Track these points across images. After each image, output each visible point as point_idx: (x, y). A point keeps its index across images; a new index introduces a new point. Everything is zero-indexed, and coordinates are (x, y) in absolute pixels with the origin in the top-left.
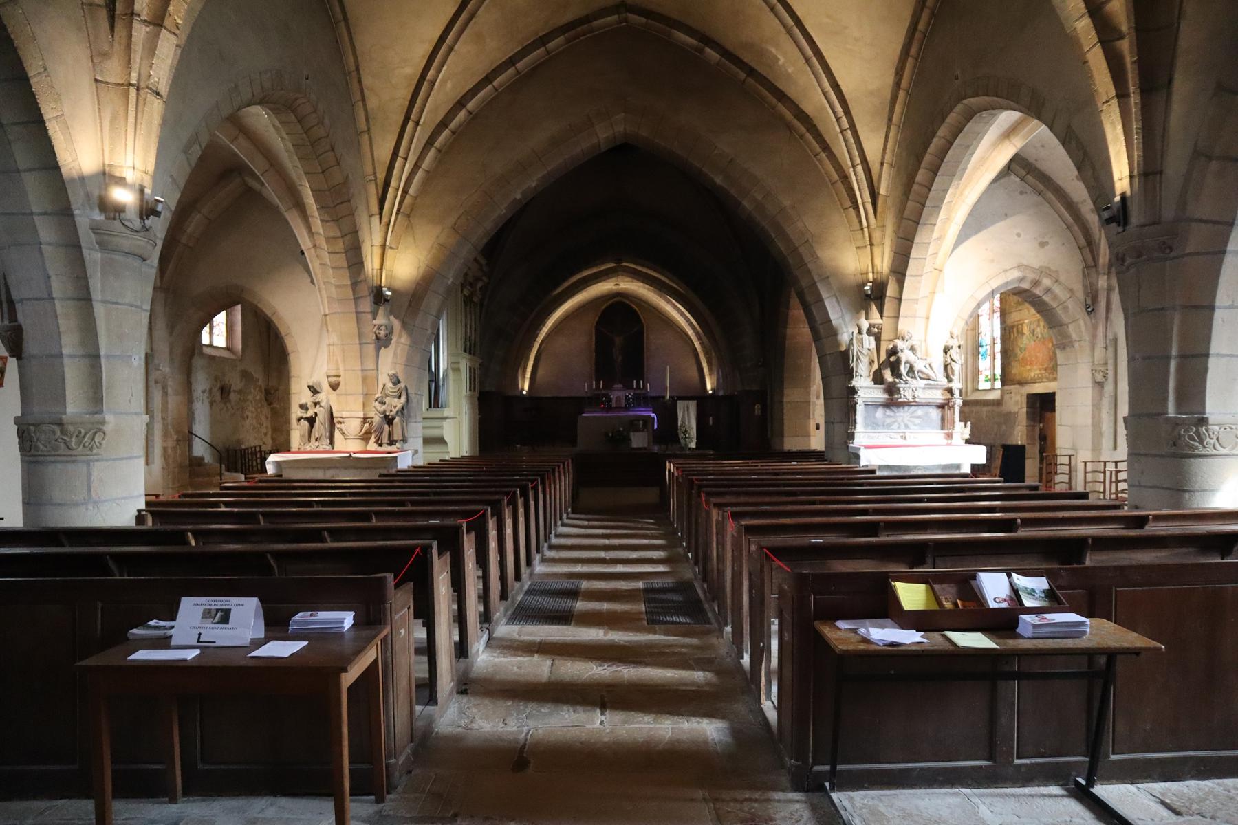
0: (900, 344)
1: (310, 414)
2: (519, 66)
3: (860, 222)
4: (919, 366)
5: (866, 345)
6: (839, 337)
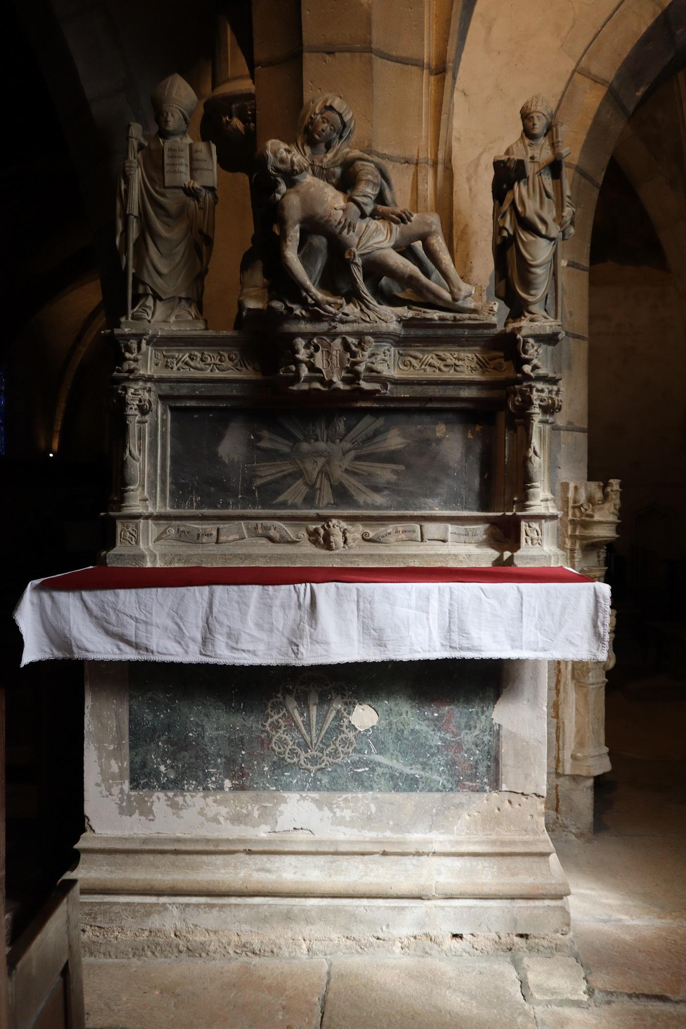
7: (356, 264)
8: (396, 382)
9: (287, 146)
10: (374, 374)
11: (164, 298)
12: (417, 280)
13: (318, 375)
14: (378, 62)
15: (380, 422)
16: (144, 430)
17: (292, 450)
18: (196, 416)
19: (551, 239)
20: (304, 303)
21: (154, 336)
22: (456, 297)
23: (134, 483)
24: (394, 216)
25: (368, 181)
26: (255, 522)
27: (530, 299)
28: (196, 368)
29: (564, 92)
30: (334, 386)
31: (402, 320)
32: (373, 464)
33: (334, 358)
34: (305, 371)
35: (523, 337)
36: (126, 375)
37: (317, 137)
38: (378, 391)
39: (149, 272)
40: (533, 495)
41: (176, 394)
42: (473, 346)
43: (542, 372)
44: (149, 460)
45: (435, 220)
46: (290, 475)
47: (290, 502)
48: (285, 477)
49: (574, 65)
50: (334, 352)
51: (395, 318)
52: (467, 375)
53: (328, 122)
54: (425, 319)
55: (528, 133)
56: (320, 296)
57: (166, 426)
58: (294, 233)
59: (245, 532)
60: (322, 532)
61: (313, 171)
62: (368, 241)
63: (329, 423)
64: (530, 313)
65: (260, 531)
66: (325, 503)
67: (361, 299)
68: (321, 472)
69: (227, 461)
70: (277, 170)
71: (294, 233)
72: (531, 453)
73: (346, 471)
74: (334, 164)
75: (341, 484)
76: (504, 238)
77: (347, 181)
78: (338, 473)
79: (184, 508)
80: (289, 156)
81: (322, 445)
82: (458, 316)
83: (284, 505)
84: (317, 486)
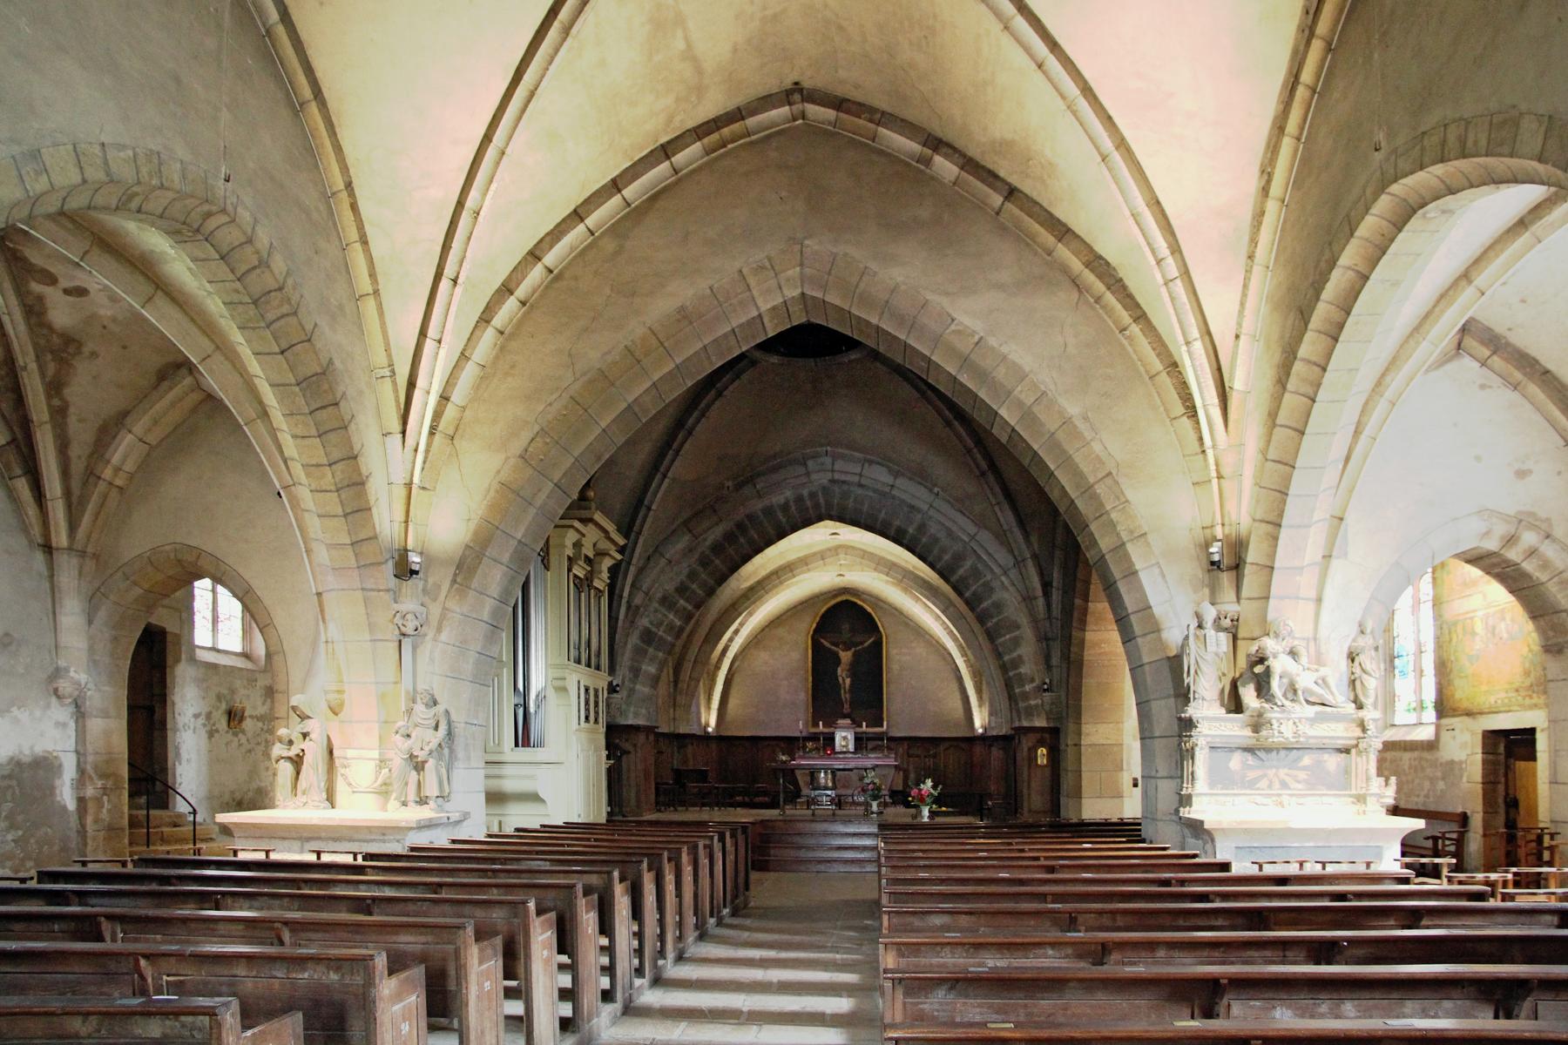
0: (1270, 644)
1: (293, 752)
2: (628, 192)
3: (1201, 439)
4: (1305, 681)
5: (1211, 648)
6: (1165, 635)
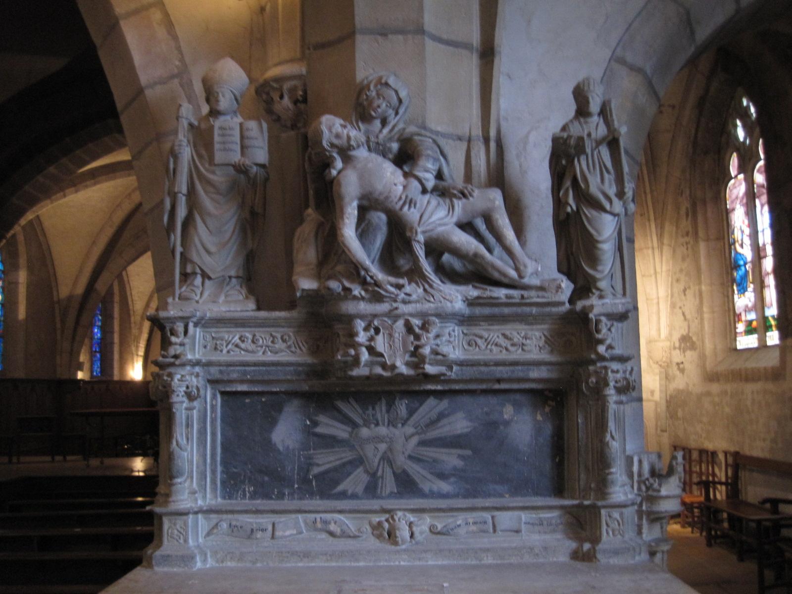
4: (435, 219)
7: (418, 242)
8: (461, 364)
9: (342, 122)
10: (440, 357)
11: (212, 276)
12: (482, 257)
13: (379, 359)
14: (430, 44)
15: (444, 404)
16: (192, 416)
17: (351, 436)
18: (247, 405)
19: (614, 215)
20: (364, 283)
21: (202, 318)
22: (523, 274)
23: (182, 475)
24: (455, 192)
25: (428, 156)
26: (312, 516)
27: (598, 276)
28: (246, 351)
29: (603, 77)
30: (397, 371)
31: (467, 299)
32: (438, 450)
33: (396, 340)
34: (365, 356)
35: (595, 316)
36: (172, 360)
37: (373, 113)
38: (444, 375)
39: (197, 251)
40: (612, 482)
41: (225, 378)
42: (541, 324)
43: (618, 351)
44: (198, 450)
45: (496, 197)
46: (350, 462)
47: (350, 492)
48: (344, 465)
49: (610, 54)
50: (397, 335)
51: (460, 298)
52: (535, 354)
53: (384, 98)
54: (491, 298)
55: (582, 112)
56: (380, 276)
57: (216, 412)
58: (351, 213)
59: (302, 525)
60: (386, 525)
61: (369, 147)
62: (430, 217)
63: (390, 406)
64: (598, 289)
65: (319, 525)
66: (388, 492)
67: (424, 278)
68: (383, 458)
69: (281, 448)
70: (332, 145)
71: (351, 213)
72: (608, 438)
73: (410, 457)
74: (391, 139)
75: (404, 471)
76: (568, 214)
77: (405, 157)
78: (401, 461)
79: (236, 499)
80: (345, 132)
81: (383, 430)
82: (525, 293)
83: (343, 495)
84: (379, 473)
